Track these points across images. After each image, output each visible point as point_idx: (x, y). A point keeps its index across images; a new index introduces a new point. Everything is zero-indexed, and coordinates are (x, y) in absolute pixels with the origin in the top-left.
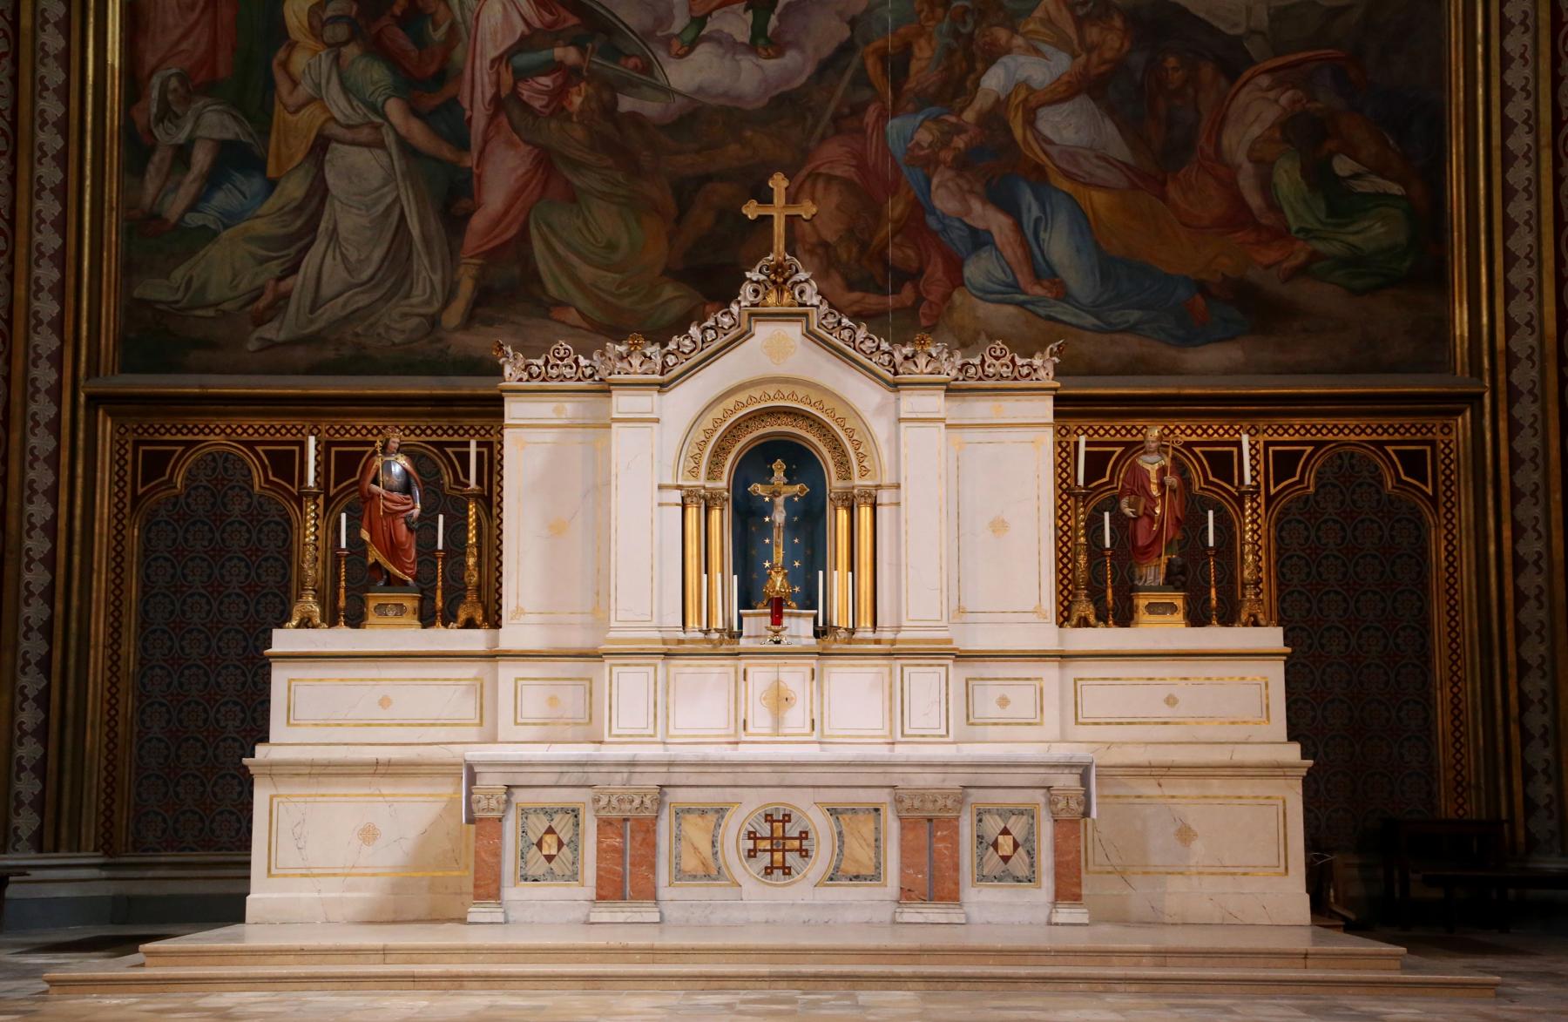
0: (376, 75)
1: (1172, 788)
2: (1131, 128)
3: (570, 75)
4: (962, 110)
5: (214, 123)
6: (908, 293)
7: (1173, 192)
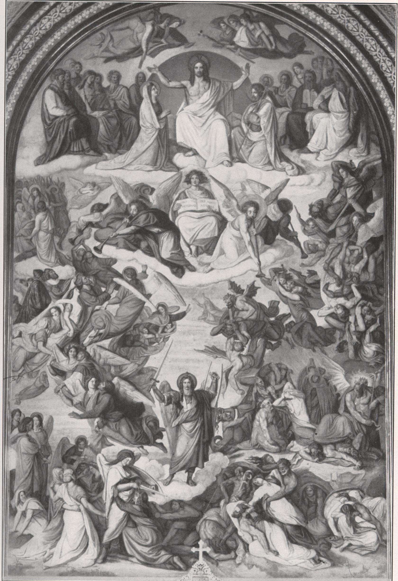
3: (134, 490)
6: (233, 554)
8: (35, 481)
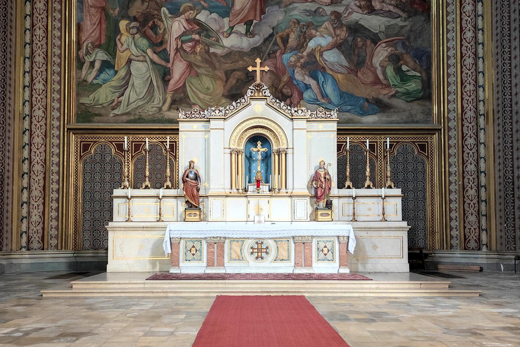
0: (143, 42)
1: (371, 233)
2: (348, 57)
3: (197, 42)
4: (303, 52)
5: (101, 56)
7: (359, 74)
8: (103, 33)
